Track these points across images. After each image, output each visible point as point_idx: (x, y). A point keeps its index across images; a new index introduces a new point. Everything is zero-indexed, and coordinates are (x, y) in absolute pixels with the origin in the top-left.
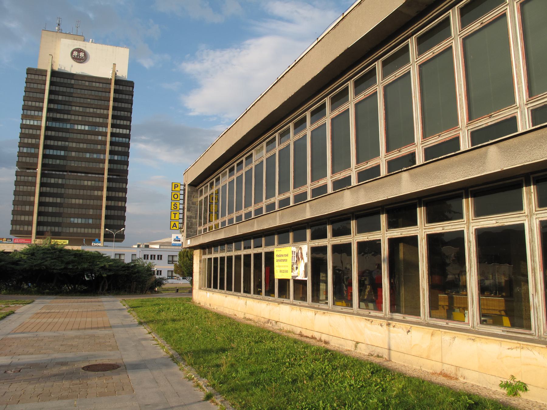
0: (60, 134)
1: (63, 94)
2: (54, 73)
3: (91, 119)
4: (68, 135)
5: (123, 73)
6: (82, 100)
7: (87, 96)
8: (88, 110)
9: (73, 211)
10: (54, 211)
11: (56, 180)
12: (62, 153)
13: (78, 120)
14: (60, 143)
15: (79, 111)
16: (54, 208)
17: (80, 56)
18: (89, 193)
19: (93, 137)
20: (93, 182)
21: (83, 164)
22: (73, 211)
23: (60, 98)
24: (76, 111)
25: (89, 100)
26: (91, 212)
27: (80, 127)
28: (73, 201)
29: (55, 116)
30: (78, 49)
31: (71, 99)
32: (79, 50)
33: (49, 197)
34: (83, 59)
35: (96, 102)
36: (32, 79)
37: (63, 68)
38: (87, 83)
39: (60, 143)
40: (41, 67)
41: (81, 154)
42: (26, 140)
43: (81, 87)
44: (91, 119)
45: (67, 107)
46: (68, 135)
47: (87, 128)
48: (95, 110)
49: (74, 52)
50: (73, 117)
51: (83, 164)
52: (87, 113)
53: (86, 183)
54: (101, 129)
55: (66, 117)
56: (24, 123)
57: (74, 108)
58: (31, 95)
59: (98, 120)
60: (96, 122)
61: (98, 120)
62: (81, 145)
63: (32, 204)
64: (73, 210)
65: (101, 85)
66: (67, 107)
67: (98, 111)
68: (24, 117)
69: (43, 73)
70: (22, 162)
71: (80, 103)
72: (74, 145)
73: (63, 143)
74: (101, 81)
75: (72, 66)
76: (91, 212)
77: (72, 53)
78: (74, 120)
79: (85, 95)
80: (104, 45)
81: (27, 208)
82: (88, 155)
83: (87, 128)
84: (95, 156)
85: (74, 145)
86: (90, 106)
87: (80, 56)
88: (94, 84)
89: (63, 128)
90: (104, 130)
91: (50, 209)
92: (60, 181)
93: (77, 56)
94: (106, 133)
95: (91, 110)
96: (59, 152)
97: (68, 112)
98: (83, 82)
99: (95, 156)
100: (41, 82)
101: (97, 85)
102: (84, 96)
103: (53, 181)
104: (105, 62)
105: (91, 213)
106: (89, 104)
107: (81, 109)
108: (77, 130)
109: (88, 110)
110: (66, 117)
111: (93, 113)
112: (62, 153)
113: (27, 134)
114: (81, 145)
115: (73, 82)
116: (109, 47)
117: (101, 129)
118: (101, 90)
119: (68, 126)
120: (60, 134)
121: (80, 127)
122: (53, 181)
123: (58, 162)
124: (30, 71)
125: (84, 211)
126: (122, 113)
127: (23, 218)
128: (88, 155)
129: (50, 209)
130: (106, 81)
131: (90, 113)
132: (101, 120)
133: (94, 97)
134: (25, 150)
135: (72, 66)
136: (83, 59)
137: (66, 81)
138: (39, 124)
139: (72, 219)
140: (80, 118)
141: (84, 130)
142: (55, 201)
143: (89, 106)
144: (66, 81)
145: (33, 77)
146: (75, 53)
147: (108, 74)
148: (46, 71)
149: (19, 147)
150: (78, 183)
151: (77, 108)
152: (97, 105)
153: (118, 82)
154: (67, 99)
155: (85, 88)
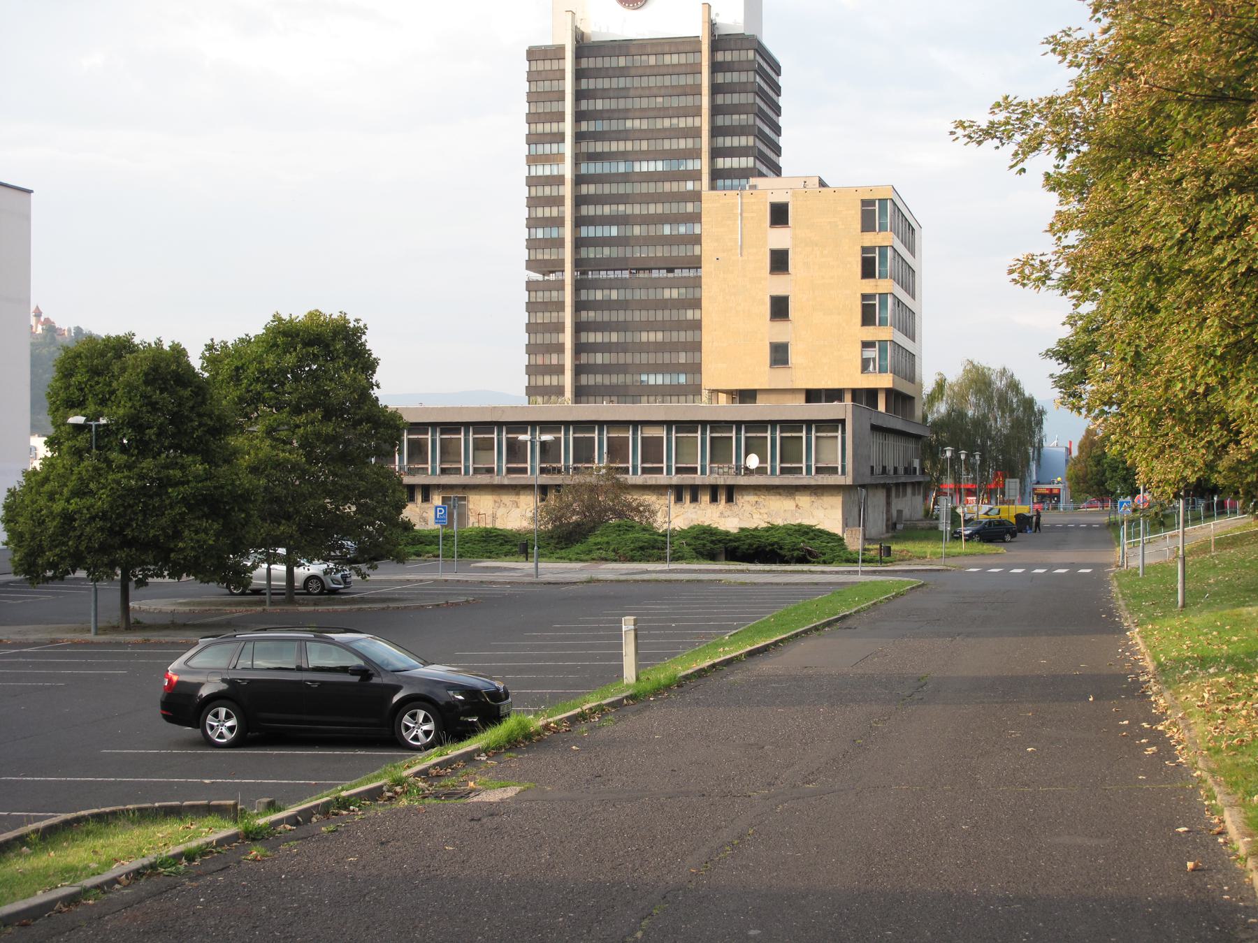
0: (607, 189)
2: (583, 47)
3: (667, 145)
4: (621, 189)
6: (645, 103)
7: (655, 91)
9: (644, 358)
10: (607, 361)
11: (606, 292)
12: (614, 231)
14: (607, 210)
15: (641, 130)
16: (607, 355)
18: (675, 315)
19: (675, 187)
20: (683, 291)
21: (660, 252)
22: (644, 358)
24: (634, 130)
25: (660, 100)
26: (682, 358)
27: (645, 167)
28: (644, 337)
29: (591, 150)
31: (622, 104)
33: (595, 331)
35: (675, 102)
36: (539, 72)
38: (652, 60)
39: (607, 210)
41: (652, 228)
42: (540, 212)
43: (640, 72)
44: (667, 145)
46: (621, 189)
47: (660, 166)
48: (675, 121)
51: (660, 252)
53: (667, 294)
54: (690, 165)
55: (614, 146)
56: (533, 173)
57: (629, 124)
59: (682, 144)
60: (679, 150)
61: (682, 144)
62: (652, 209)
63: (560, 349)
64: (644, 356)
65: (683, 59)
68: (532, 160)
69: (556, 53)
70: (536, 260)
71: (641, 109)
72: (638, 209)
73: (614, 207)
74: (682, 48)
76: (682, 358)
78: (633, 152)
79: (649, 88)
81: (554, 359)
82: (667, 230)
83: (660, 166)
84: (682, 229)
85: (638, 209)
86: (664, 113)
88: (667, 59)
91: (599, 358)
92: (614, 295)
94: (700, 171)
96: (606, 228)
99: (682, 229)
100: (558, 75)
101: (675, 59)
102: (647, 92)
103: (599, 295)
105: (682, 361)
107: (645, 124)
108: (641, 173)
110: (614, 146)
112: (614, 231)
113: (540, 195)
114: (652, 209)
115: (622, 62)
117: (690, 165)
118: (683, 70)
120: (607, 189)
121: (645, 167)
122: (599, 295)
123: (607, 251)
125: (667, 358)
126: (736, 117)
127: (547, 380)
128: (667, 230)
129: (599, 358)
131: (664, 130)
132: (690, 143)
133: (670, 91)
134: (540, 233)
137: (608, 62)
139: (644, 377)
140: (644, 145)
141: (656, 172)
142: (606, 340)
143: (662, 114)
144: (608, 62)
145: (540, 66)
147: (695, 28)
149: (529, 227)
150: (652, 294)
151: (637, 123)
152: (678, 108)
153: (719, 41)
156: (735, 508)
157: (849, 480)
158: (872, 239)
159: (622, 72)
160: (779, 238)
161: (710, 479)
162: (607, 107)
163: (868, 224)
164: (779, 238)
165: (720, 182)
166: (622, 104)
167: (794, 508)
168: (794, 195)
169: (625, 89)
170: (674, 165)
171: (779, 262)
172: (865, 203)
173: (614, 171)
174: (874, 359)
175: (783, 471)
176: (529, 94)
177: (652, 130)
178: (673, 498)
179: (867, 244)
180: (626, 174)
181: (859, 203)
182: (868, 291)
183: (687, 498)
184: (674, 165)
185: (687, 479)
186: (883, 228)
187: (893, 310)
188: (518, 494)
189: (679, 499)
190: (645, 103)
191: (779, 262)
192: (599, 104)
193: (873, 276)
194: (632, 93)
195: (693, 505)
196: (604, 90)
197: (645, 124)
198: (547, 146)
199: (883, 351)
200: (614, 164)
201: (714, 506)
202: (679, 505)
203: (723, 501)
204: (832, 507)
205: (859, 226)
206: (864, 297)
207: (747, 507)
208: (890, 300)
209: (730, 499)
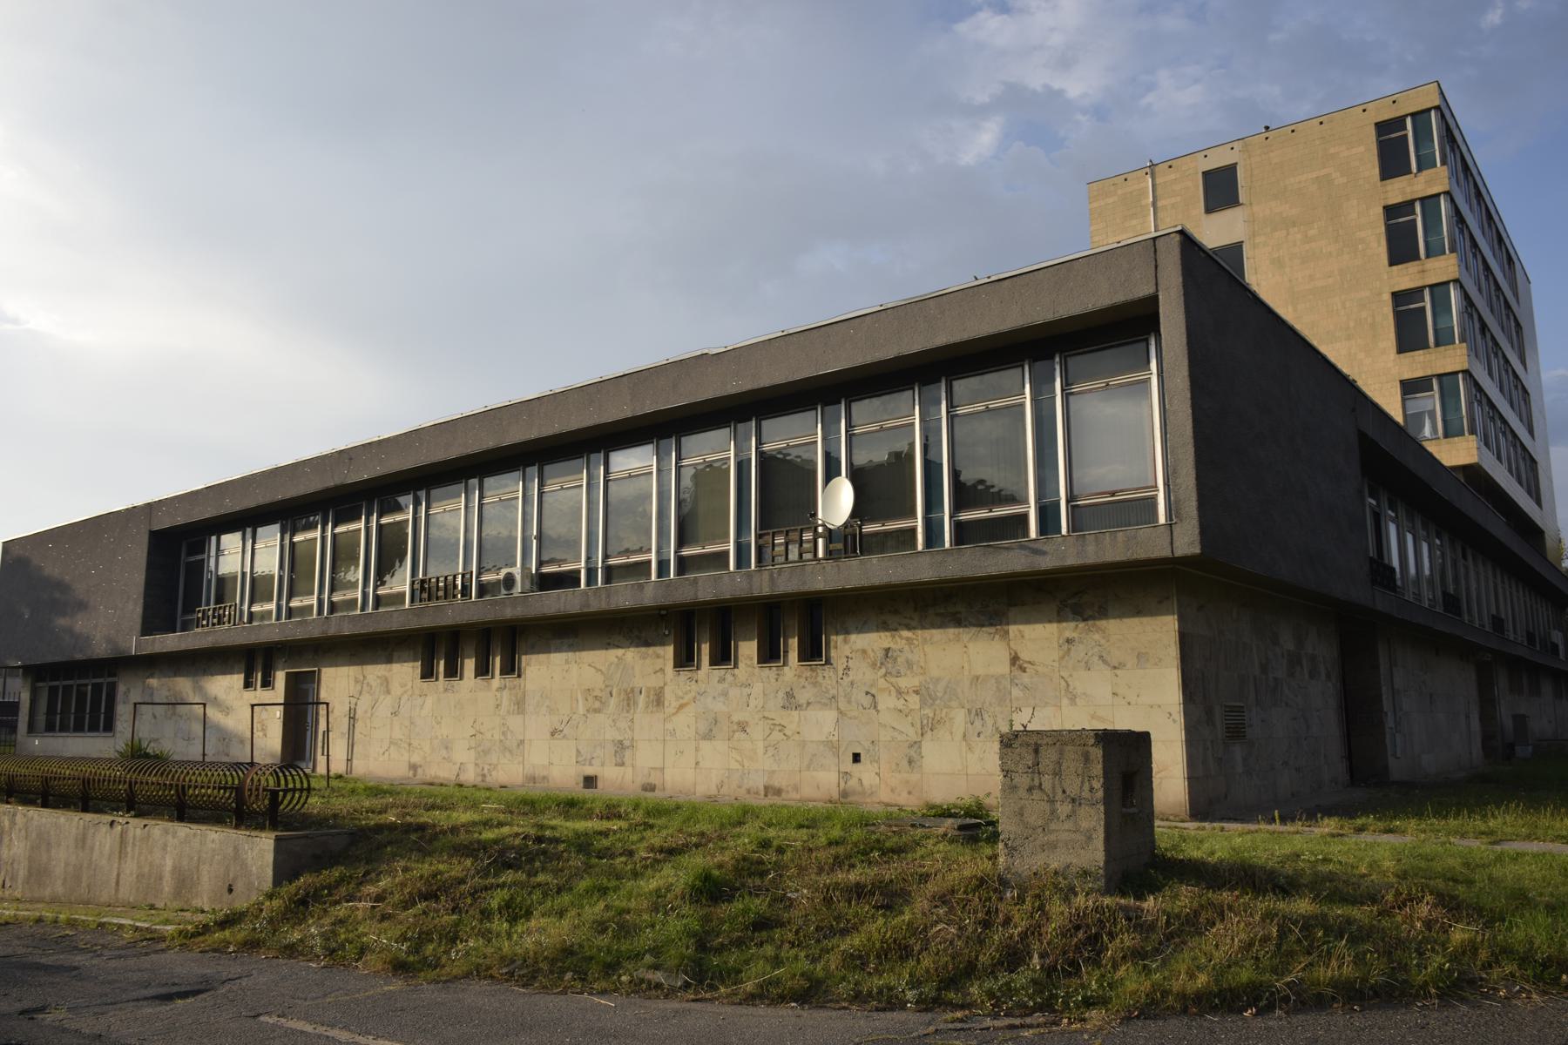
156: (826, 676)
157: (1187, 542)
158: (1399, 190)
161: (763, 586)
163: (1392, 161)
167: (1004, 668)
172: (1383, 128)
174: (1432, 414)
175: (963, 533)
178: (669, 651)
181: (1372, 133)
183: (748, 649)
185: (706, 587)
186: (1425, 163)
187: (1460, 314)
189: (685, 659)
193: (1417, 258)
195: (718, 672)
199: (1448, 396)
201: (769, 672)
202: (685, 674)
203: (793, 655)
204: (1141, 658)
205: (1377, 171)
206: (1399, 297)
207: (862, 673)
208: (1454, 294)
209: (813, 651)
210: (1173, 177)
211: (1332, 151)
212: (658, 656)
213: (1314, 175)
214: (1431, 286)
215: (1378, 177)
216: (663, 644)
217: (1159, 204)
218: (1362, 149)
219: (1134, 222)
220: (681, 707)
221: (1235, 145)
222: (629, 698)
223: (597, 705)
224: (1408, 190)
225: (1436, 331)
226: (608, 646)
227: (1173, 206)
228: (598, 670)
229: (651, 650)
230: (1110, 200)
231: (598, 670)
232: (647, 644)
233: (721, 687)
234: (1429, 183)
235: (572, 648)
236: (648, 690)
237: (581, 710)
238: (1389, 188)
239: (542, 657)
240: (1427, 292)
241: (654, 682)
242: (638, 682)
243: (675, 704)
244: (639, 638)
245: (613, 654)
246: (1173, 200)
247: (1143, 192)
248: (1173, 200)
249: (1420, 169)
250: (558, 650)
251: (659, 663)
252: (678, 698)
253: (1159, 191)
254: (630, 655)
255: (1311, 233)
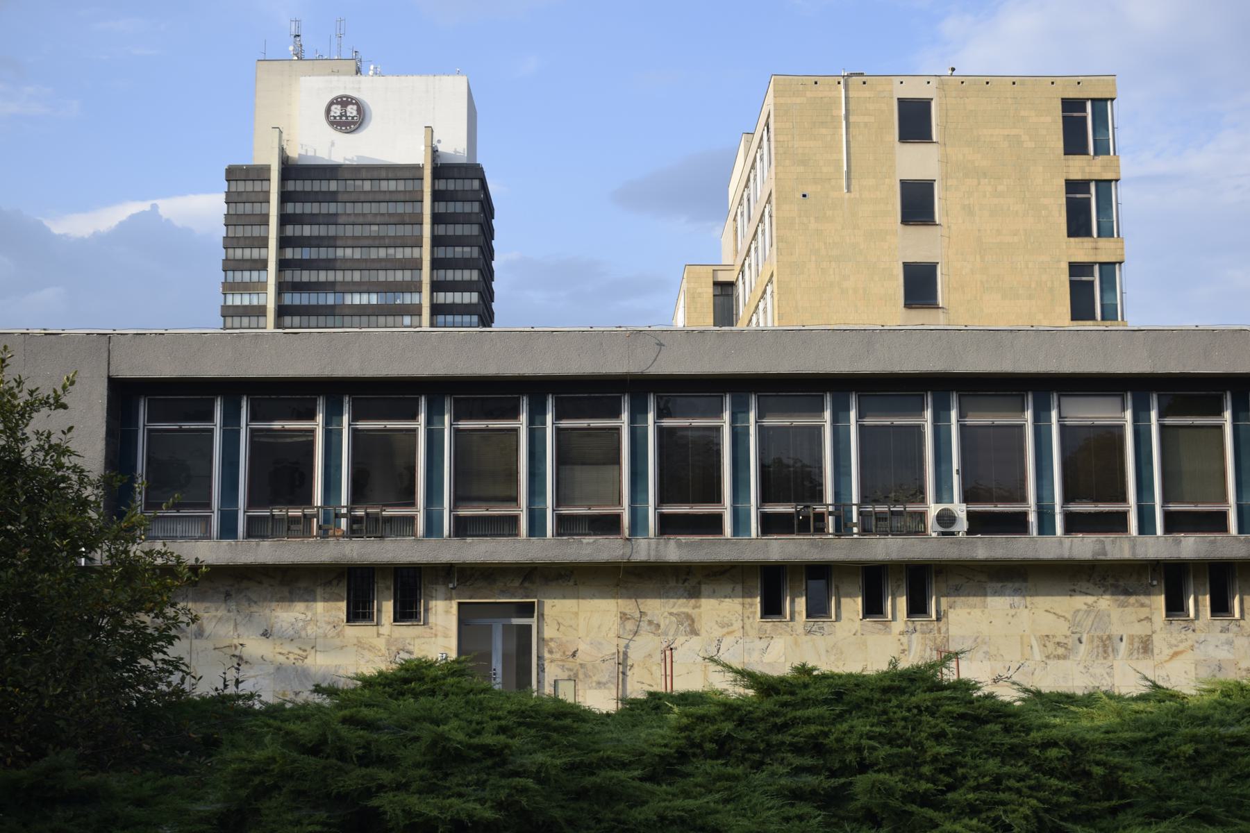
1: (312, 219)
2: (290, 170)
3: (381, 276)
5: (454, 146)
6: (358, 230)
7: (370, 219)
8: (374, 254)
13: (353, 283)
15: (352, 260)
17: (347, 116)
23: (307, 231)
24: (344, 260)
25: (375, 228)
27: (357, 299)
29: (297, 279)
30: (341, 97)
31: (332, 230)
32: (344, 101)
34: (354, 123)
35: (391, 231)
36: (239, 193)
37: (311, 153)
38: (367, 186)
40: (258, 160)
43: (353, 197)
44: (381, 276)
45: (324, 253)
47: (374, 299)
48: (391, 251)
49: (333, 108)
50: (339, 276)
52: (373, 260)
54: (408, 299)
55: (323, 276)
56: (229, 303)
58: (240, 231)
59: (399, 276)
60: (395, 283)
61: (399, 276)
65: (401, 186)
66: (324, 253)
67: (400, 253)
68: (229, 288)
69: (260, 173)
71: (354, 237)
74: (400, 174)
75: (333, 144)
77: (328, 111)
78: (343, 283)
79: (364, 215)
80: (403, 78)
83: (374, 299)
86: (379, 242)
87: (347, 116)
88: (384, 185)
89: (318, 307)
90: (415, 299)
93: (341, 116)
94: (420, 306)
95: (382, 253)
97: (329, 265)
98: (359, 183)
100: (261, 197)
101: (392, 185)
102: (361, 220)
104: (408, 124)
106: (374, 238)
107: (357, 253)
108: (352, 306)
109: (374, 254)
110: (323, 276)
111: (387, 260)
115: (333, 186)
116: (416, 78)
117: (408, 299)
118: (402, 197)
119: (330, 299)
121: (357, 299)
124: (233, 174)
126: (458, 249)
130: (413, 172)
131: (379, 260)
132: (407, 275)
133: (386, 219)
135: (333, 144)
136: (354, 123)
138: (262, 303)
140: (357, 276)
141: (369, 306)
143: (377, 243)
144: (317, 186)
145: (241, 186)
146: (336, 110)
147: (416, 155)
148: (267, 169)
151: (349, 252)
152: (395, 237)
153: (442, 170)
154: (322, 231)
155: (362, 198)
159: (332, 197)
160: (917, 162)
162: (316, 233)
164: (917, 162)
165: (441, 318)
166: (332, 230)
168: (942, 87)
169: (336, 215)
170: (389, 299)
171: (917, 204)
172: (1071, 106)
173: (322, 302)
176: (227, 216)
177: (366, 260)
178: (1160, 601)
179: (1076, 175)
180: (333, 307)
182: (1081, 257)
184: (389, 299)
188: (694, 594)
189: (1175, 607)
190: (358, 230)
191: (917, 204)
192: (307, 231)
193: (1088, 233)
194: (340, 220)
195: (1220, 623)
196: (312, 215)
197: (357, 253)
198: (247, 274)
200: (322, 296)
202: (1177, 624)
205: (1061, 144)
210: (867, 94)
211: (1023, 113)
212: (1142, 605)
213: (1006, 132)
214: (1101, 264)
215: (1061, 151)
216: (1147, 593)
217: (852, 119)
218: (1049, 119)
219: (824, 131)
220: (1176, 654)
221: (932, 80)
222: (1106, 646)
223: (1060, 651)
224: (1087, 169)
225: (1102, 306)
226: (1073, 592)
227: (866, 124)
228: (1059, 617)
229: (1132, 599)
230: (798, 100)
231: (1059, 617)
232: (1127, 593)
233: (1224, 636)
234: (1104, 167)
235: (1017, 592)
236: (1132, 638)
237: (1038, 655)
238: (1071, 163)
239: (962, 598)
240: (1097, 268)
241: (1140, 630)
242: (1116, 629)
243: (1167, 652)
244: (1116, 587)
245: (1080, 602)
246: (866, 119)
247: (835, 101)
248: (866, 119)
249: (1096, 153)
250: (996, 593)
251: (1144, 612)
252: (1171, 646)
253: (852, 106)
254: (1105, 602)
255: (1000, 188)
